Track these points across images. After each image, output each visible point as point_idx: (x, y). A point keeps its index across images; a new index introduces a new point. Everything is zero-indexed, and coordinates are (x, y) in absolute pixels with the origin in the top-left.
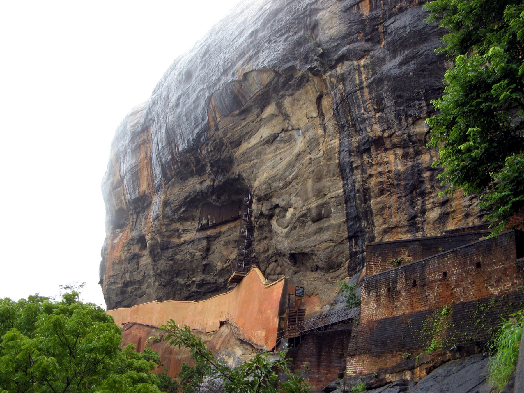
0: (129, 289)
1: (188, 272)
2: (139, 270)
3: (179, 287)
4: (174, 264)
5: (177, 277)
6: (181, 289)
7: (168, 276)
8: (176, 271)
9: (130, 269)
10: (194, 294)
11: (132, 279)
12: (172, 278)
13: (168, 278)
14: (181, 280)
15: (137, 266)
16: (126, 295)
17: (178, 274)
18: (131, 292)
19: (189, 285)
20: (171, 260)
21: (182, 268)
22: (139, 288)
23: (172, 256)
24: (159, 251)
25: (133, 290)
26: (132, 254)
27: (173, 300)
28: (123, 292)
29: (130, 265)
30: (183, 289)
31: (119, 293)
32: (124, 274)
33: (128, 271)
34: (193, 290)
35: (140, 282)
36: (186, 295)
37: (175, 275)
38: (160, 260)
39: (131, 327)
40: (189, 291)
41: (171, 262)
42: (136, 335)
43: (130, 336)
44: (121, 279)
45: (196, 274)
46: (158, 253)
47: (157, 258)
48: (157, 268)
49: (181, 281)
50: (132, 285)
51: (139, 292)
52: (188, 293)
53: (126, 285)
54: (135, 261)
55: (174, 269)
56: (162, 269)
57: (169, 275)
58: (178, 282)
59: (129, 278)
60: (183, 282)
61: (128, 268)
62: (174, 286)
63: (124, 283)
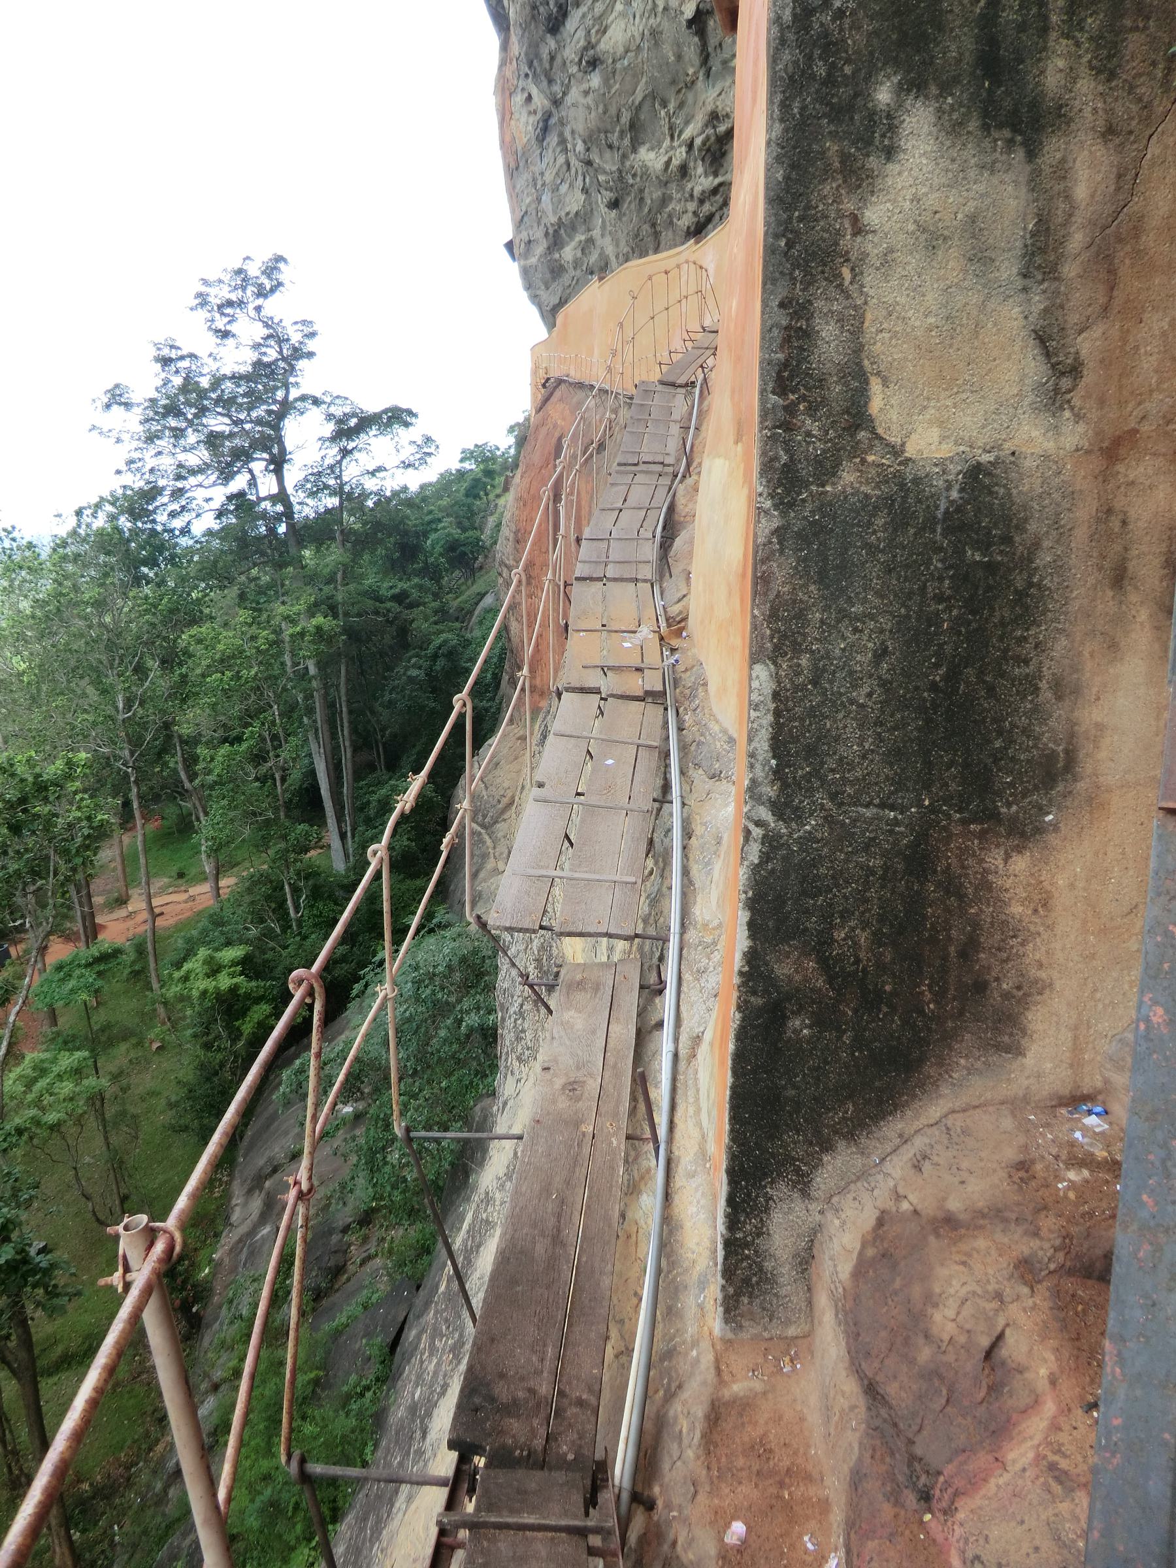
0: (568, 253)
1: (664, 104)
2: (573, 171)
3: (657, 194)
4: (606, 82)
5: (634, 150)
6: (665, 200)
7: (608, 154)
8: (626, 118)
9: (549, 177)
10: (707, 208)
11: (563, 214)
12: (624, 157)
13: (608, 163)
14: (652, 155)
15: (561, 160)
16: (566, 279)
17: (636, 132)
18: (577, 264)
19: (684, 170)
20: (594, 63)
21: (639, 96)
22: (590, 241)
23: (590, 46)
24: (552, 43)
25: (579, 254)
26: (539, 115)
27: (657, 250)
28: (557, 270)
29: (545, 160)
30: (671, 198)
31: (548, 276)
32: (539, 200)
33: (544, 185)
34: (697, 190)
35: (583, 218)
36: (687, 221)
37: (627, 141)
38: (568, 87)
39: (551, 394)
40: (692, 196)
41: (595, 80)
42: (555, 426)
43: (543, 431)
44: (539, 224)
45: (690, 97)
46: (552, 58)
47: (557, 88)
48: (573, 132)
49: (650, 158)
50: (571, 238)
51: (594, 258)
52: (692, 206)
53: (556, 241)
54: (552, 139)
55: (613, 111)
56: (580, 127)
57: (610, 147)
58: (645, 173)
59: (555, 212)
60: (659, 165)
61: (542, 174)
62: (641, 191)
63: (547, 234)
